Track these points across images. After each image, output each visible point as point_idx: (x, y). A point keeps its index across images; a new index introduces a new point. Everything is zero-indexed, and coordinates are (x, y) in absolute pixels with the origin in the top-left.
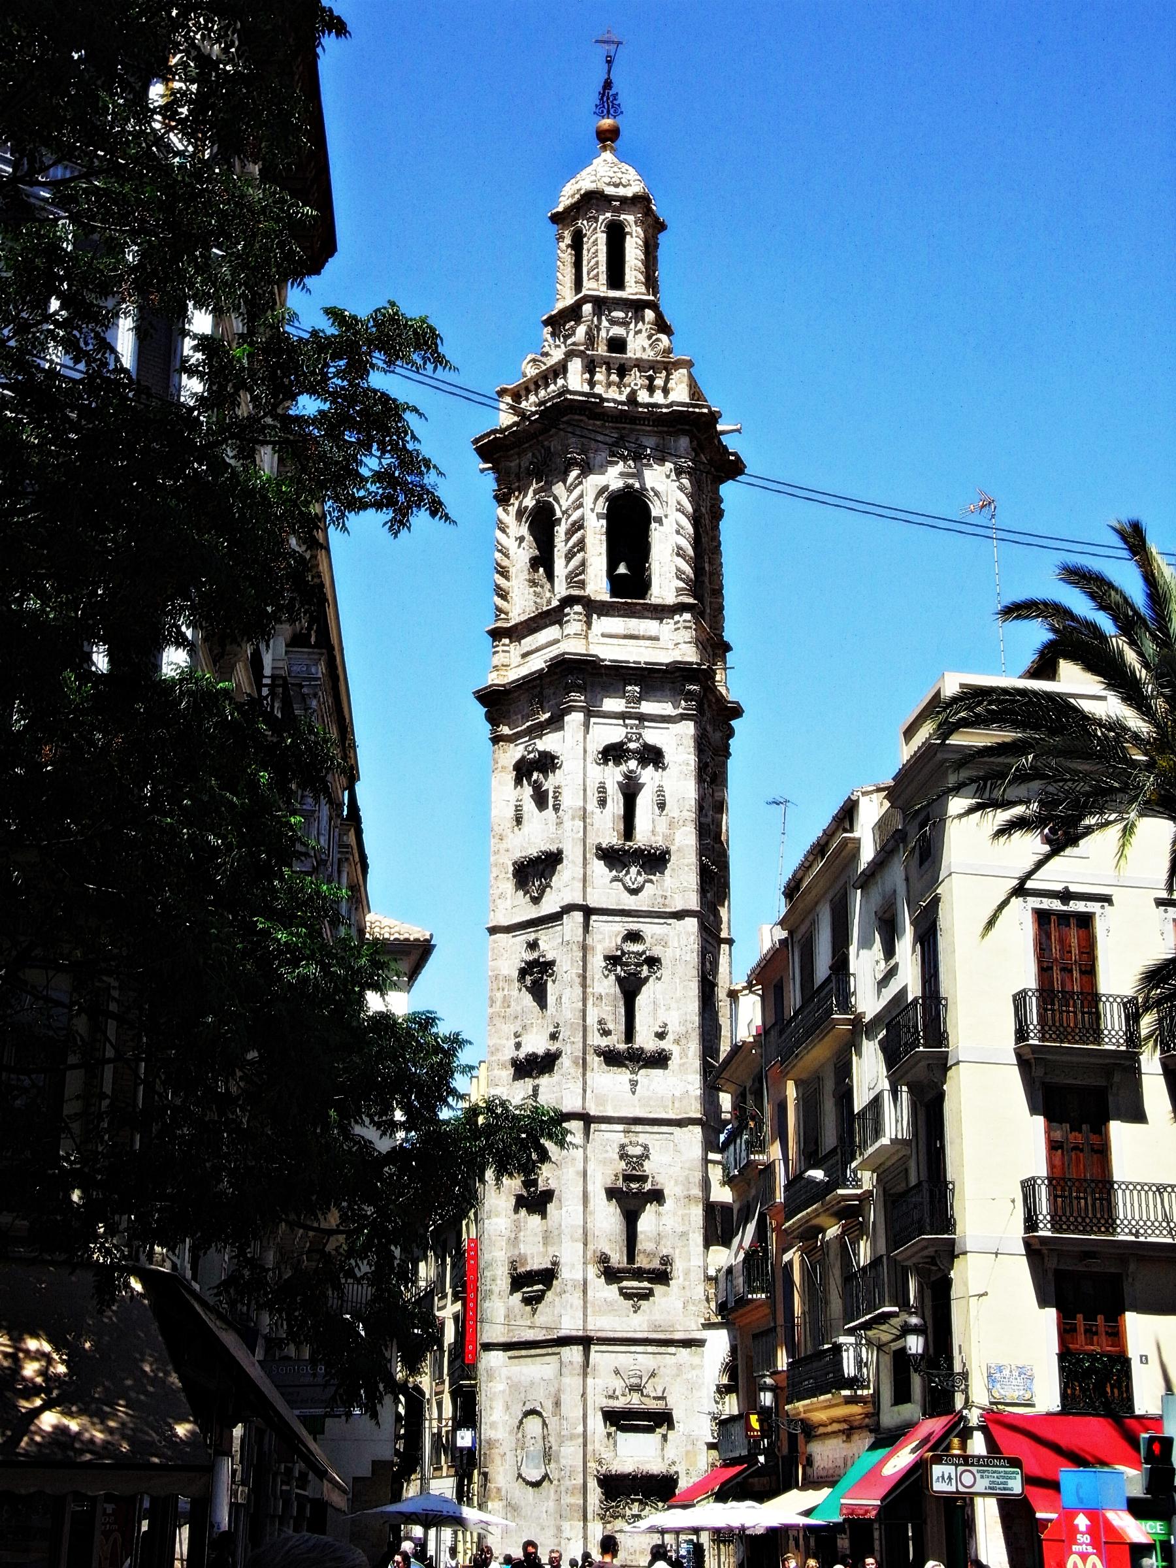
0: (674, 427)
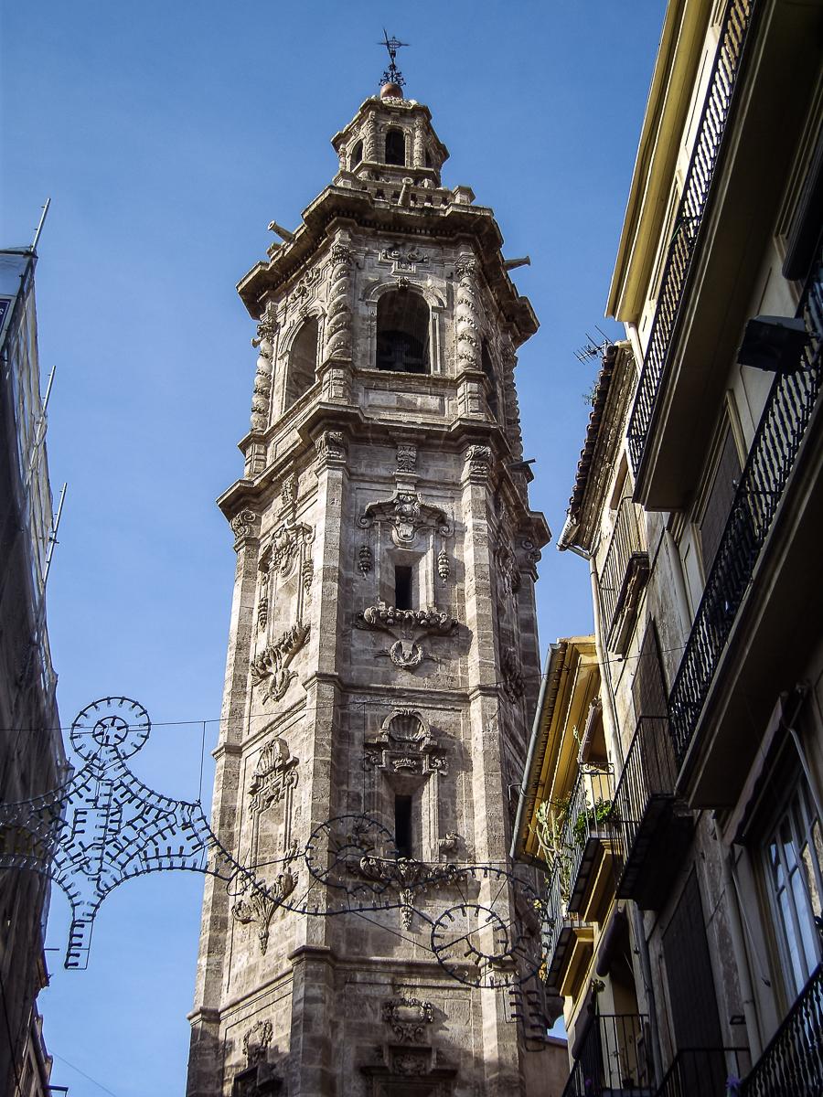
0: (451, 236)
